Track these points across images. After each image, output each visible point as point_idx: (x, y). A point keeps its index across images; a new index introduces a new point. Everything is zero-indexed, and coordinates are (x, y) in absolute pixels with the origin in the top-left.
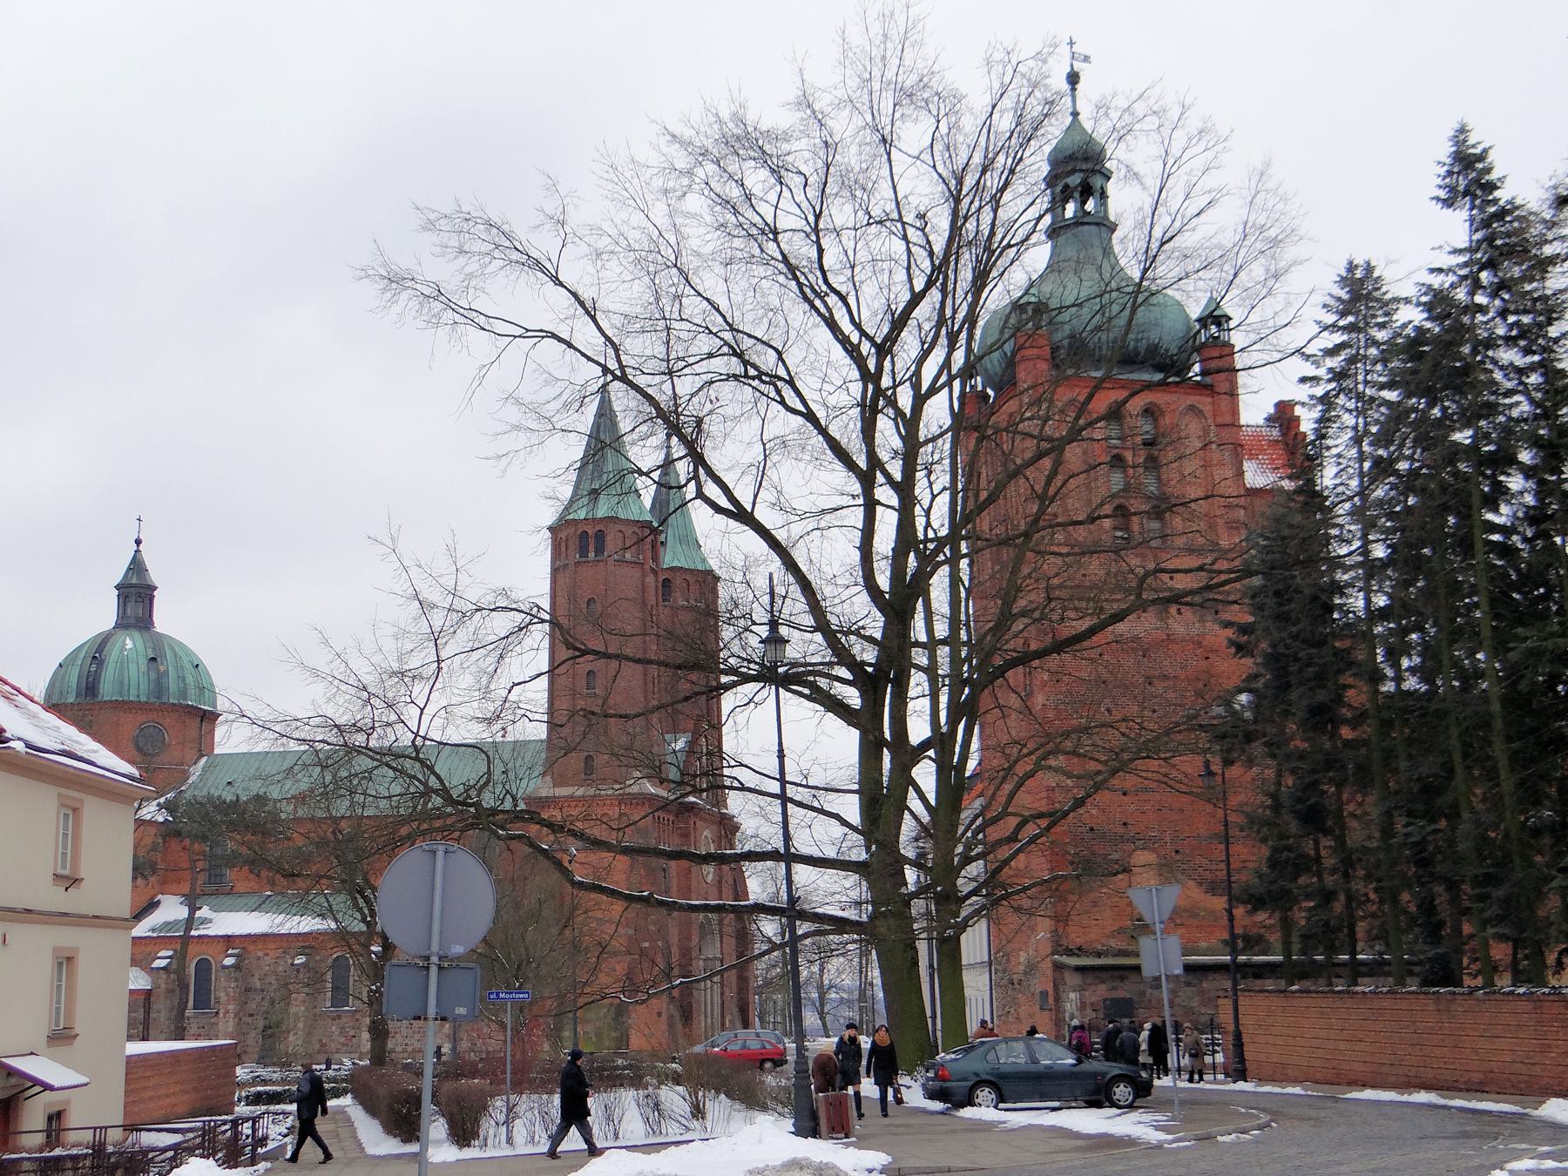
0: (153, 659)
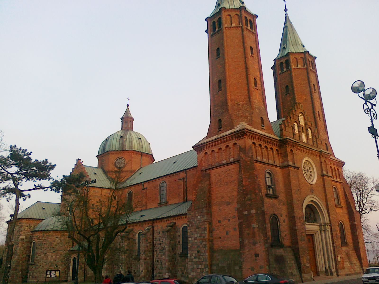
0: (121, 137)
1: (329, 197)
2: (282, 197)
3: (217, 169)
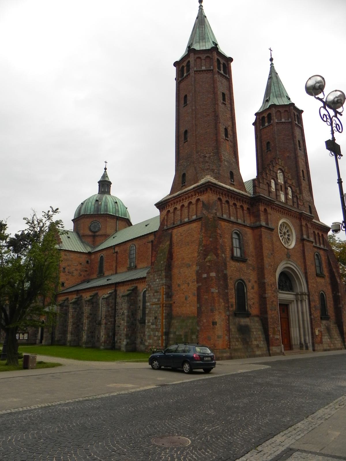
1: (309, 264)
2: (251, 260)
3: (179, 229)
